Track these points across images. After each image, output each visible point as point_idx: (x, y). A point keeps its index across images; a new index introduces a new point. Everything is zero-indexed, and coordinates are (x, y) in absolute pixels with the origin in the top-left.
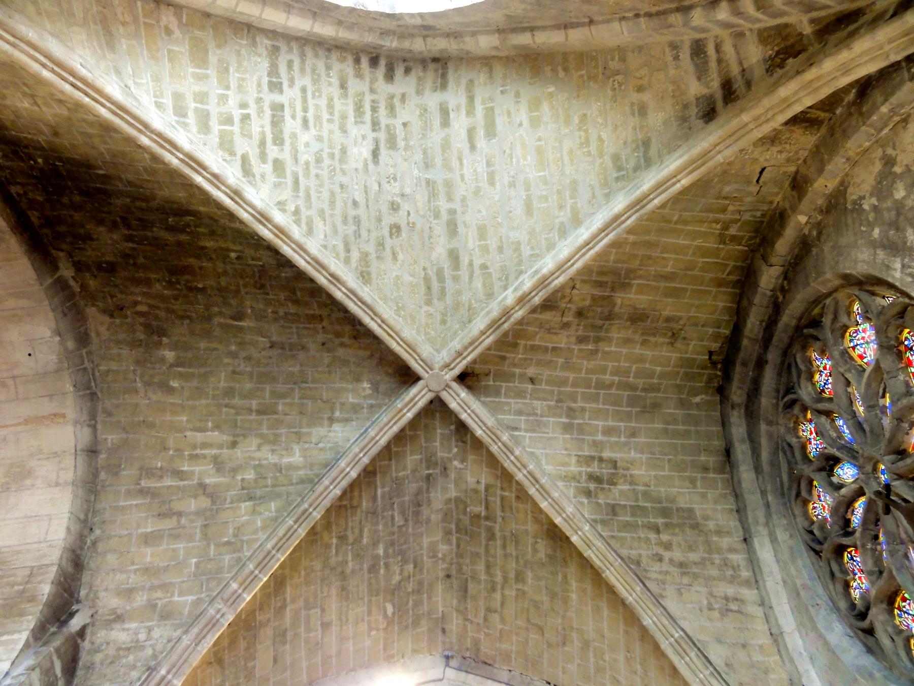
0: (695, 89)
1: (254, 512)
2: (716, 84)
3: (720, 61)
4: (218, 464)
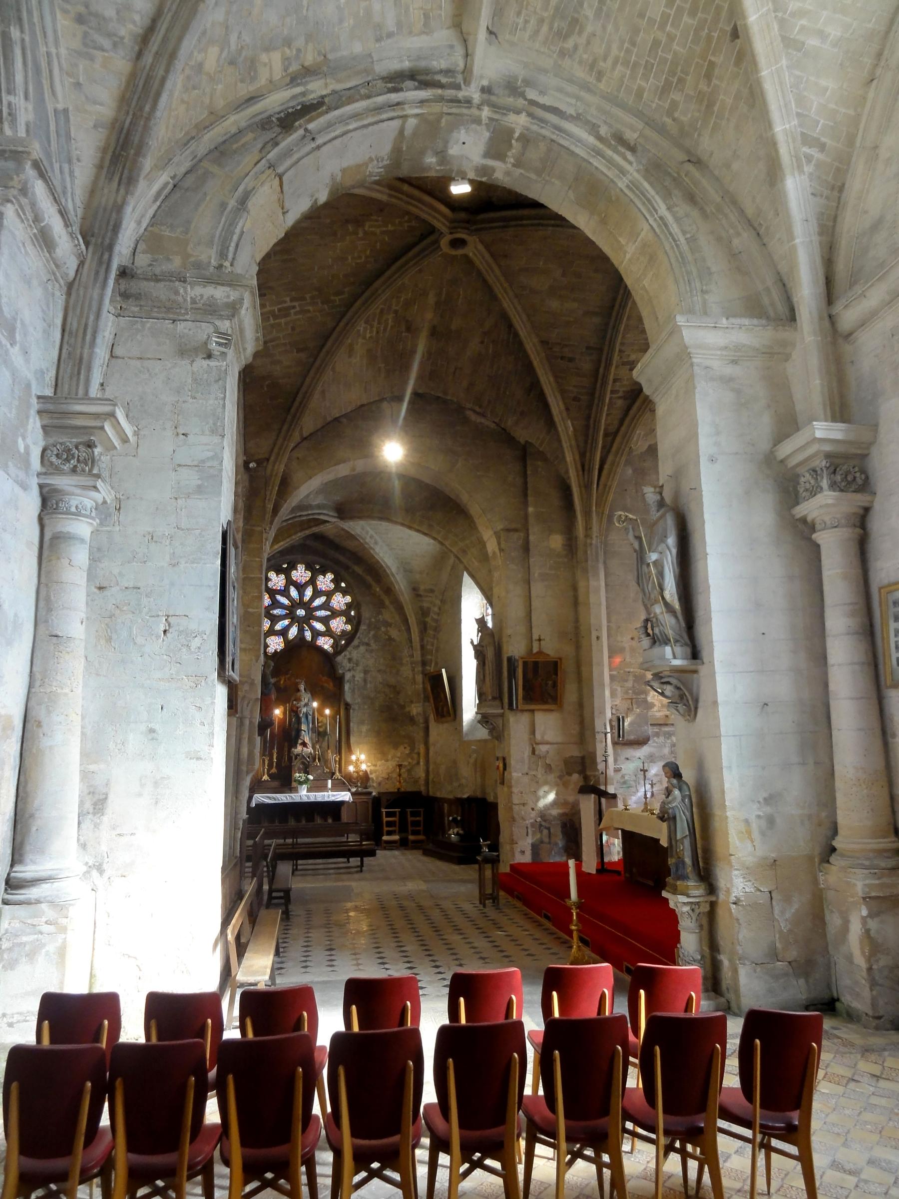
0: (422, 587)
2: (422, 593)
3: (427, 596)
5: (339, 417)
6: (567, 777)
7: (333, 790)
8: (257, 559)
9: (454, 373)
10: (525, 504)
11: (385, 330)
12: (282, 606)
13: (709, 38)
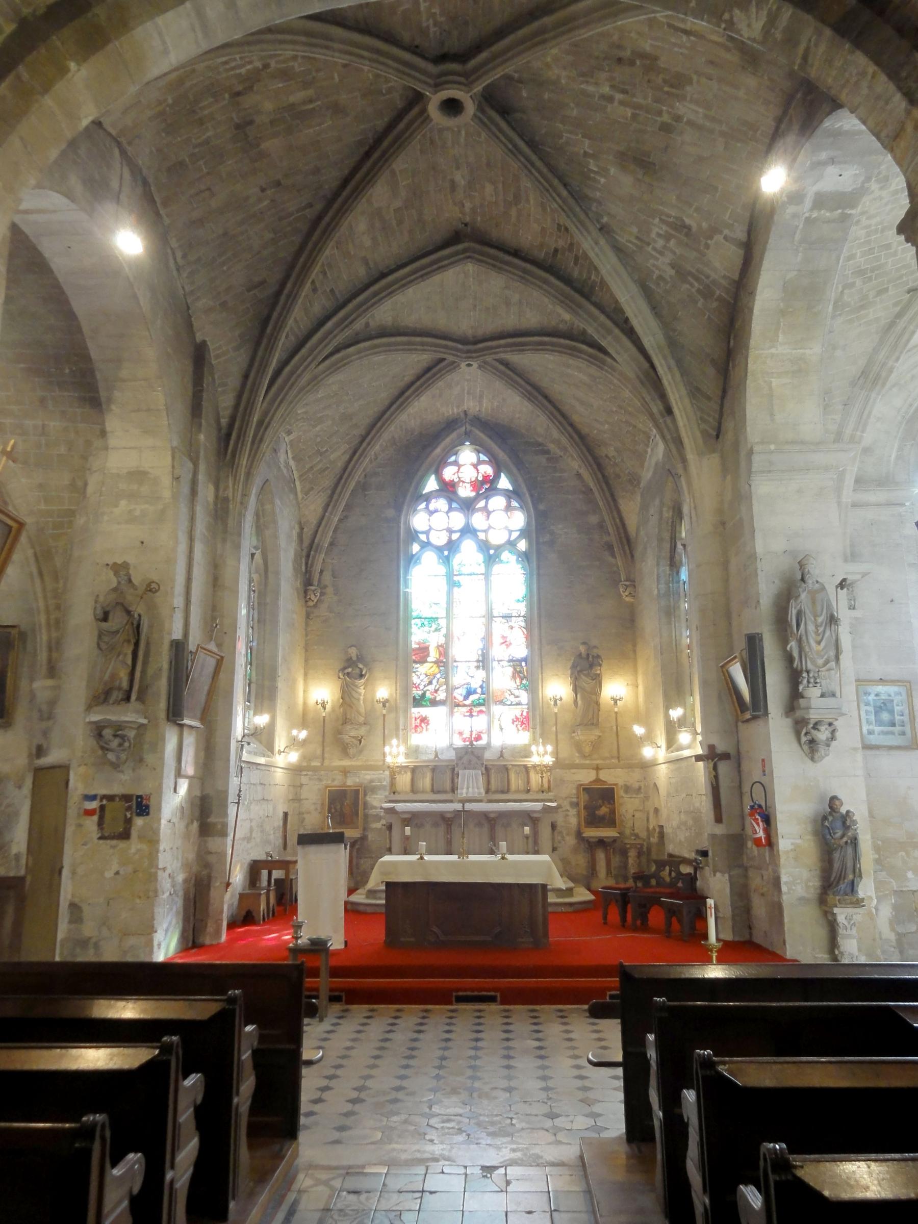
9: (201, 192)
11: (233, 69)
13: (901, 277)
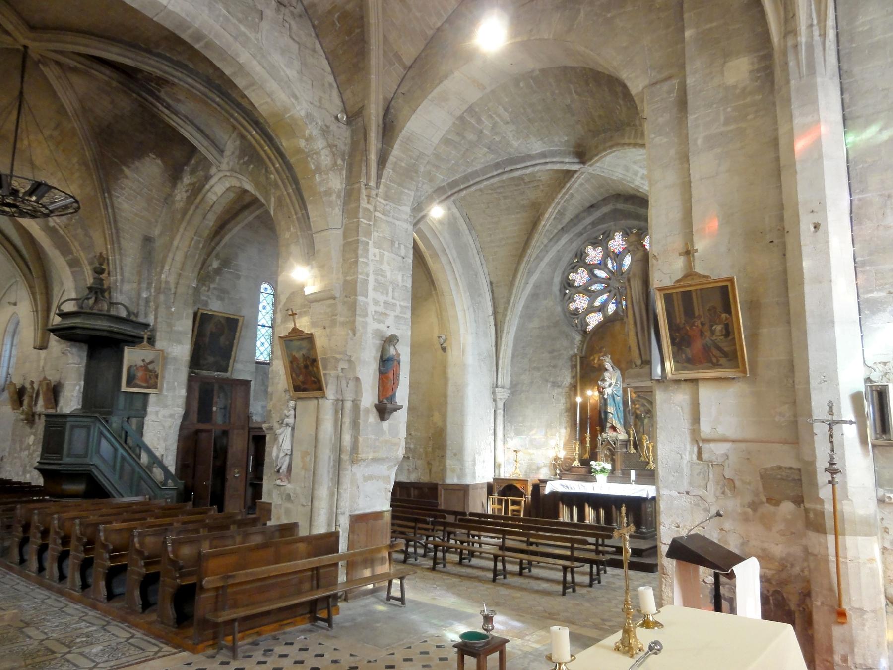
1: (485, 155)
4: (495, 126)
5: (442, 25)
6: (769, 508)
7: (638, 482)
8: (355, 220)
10: (682, 30)
12: (601, 281)
